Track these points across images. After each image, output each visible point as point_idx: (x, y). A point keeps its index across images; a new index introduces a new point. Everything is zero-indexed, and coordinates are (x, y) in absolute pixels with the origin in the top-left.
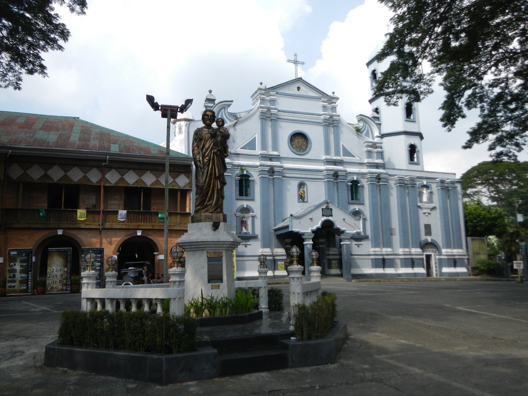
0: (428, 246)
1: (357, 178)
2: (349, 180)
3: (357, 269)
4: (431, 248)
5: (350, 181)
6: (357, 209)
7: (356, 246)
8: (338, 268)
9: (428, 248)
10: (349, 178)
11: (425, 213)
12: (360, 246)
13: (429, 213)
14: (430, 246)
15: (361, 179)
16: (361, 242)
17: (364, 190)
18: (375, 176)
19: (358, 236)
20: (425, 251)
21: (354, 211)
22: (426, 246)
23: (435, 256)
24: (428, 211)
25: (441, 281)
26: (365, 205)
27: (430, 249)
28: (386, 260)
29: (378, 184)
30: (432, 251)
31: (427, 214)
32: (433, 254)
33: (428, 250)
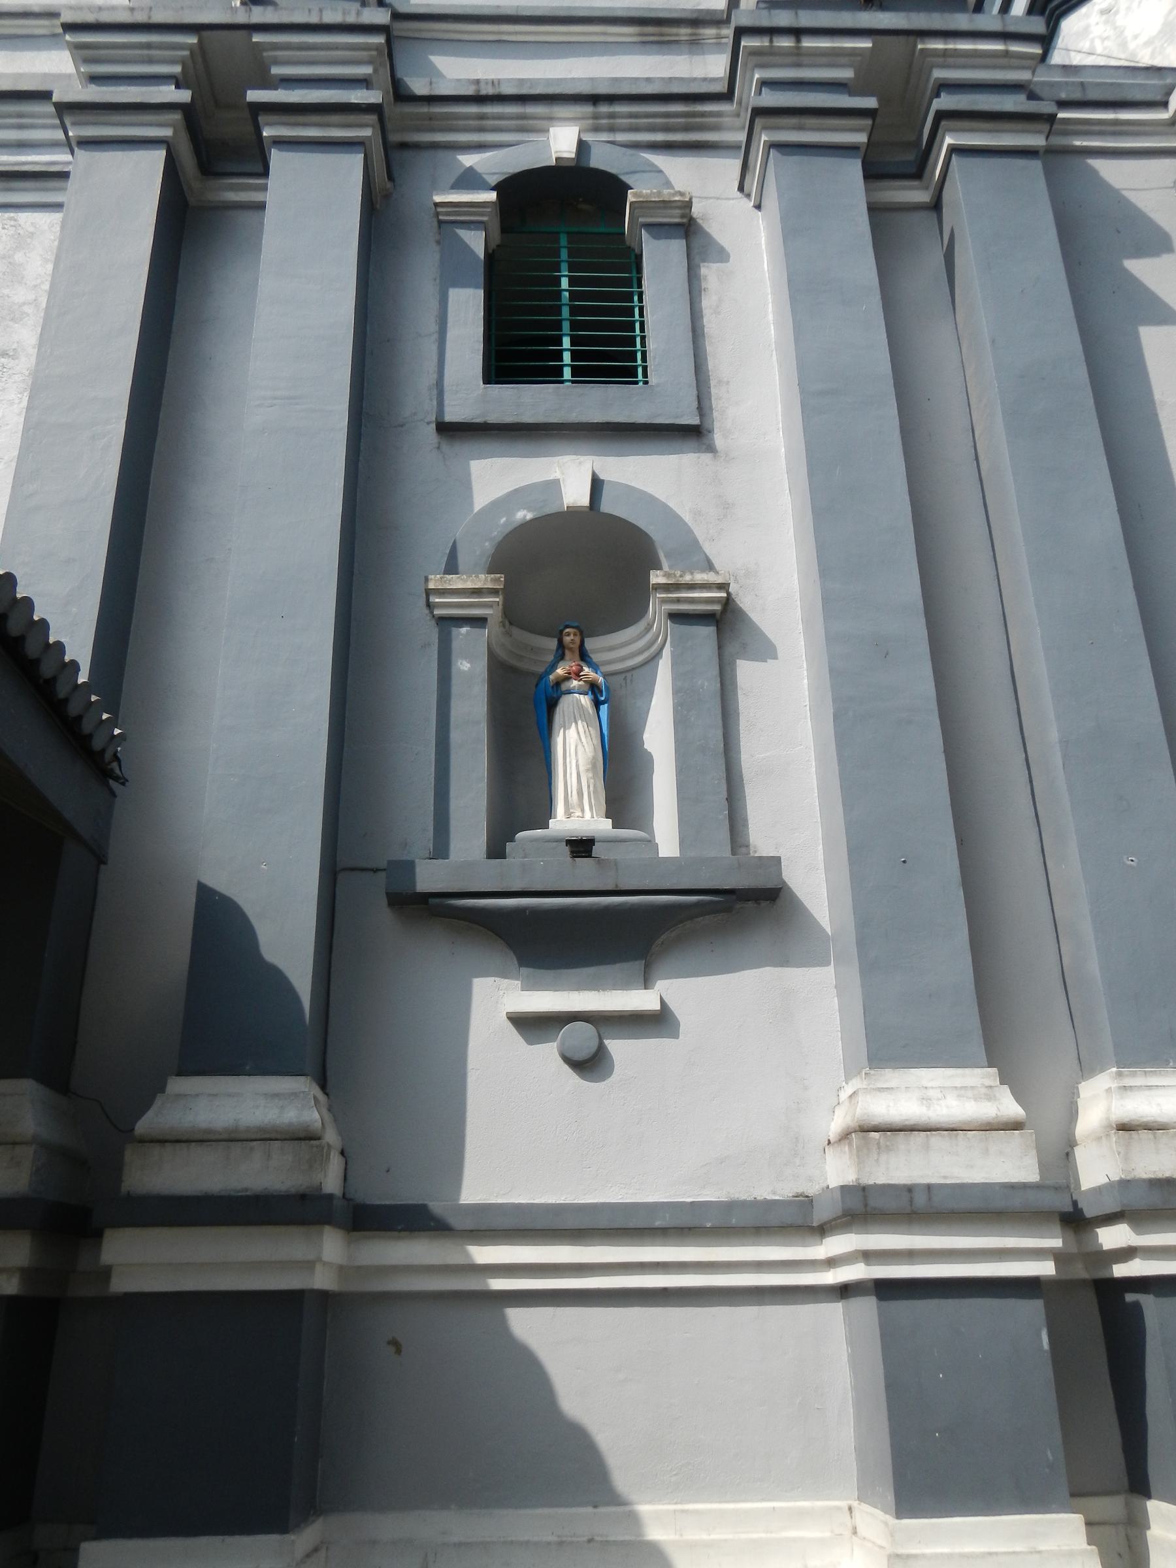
1: (582, 146)
2: (470, 170)
5: (493, 180)
6: (576, 494)
7: (548, 1054)
10: (468, 160)
12: (618, 1048)
15: (659, 160)
16: (647, 984)
17: (709, 272)
18: (847, 74)
19: (584, 874)
21: (524, 515)
26: (718, 439)
28: (1149, 1304)
29: (921, 196)
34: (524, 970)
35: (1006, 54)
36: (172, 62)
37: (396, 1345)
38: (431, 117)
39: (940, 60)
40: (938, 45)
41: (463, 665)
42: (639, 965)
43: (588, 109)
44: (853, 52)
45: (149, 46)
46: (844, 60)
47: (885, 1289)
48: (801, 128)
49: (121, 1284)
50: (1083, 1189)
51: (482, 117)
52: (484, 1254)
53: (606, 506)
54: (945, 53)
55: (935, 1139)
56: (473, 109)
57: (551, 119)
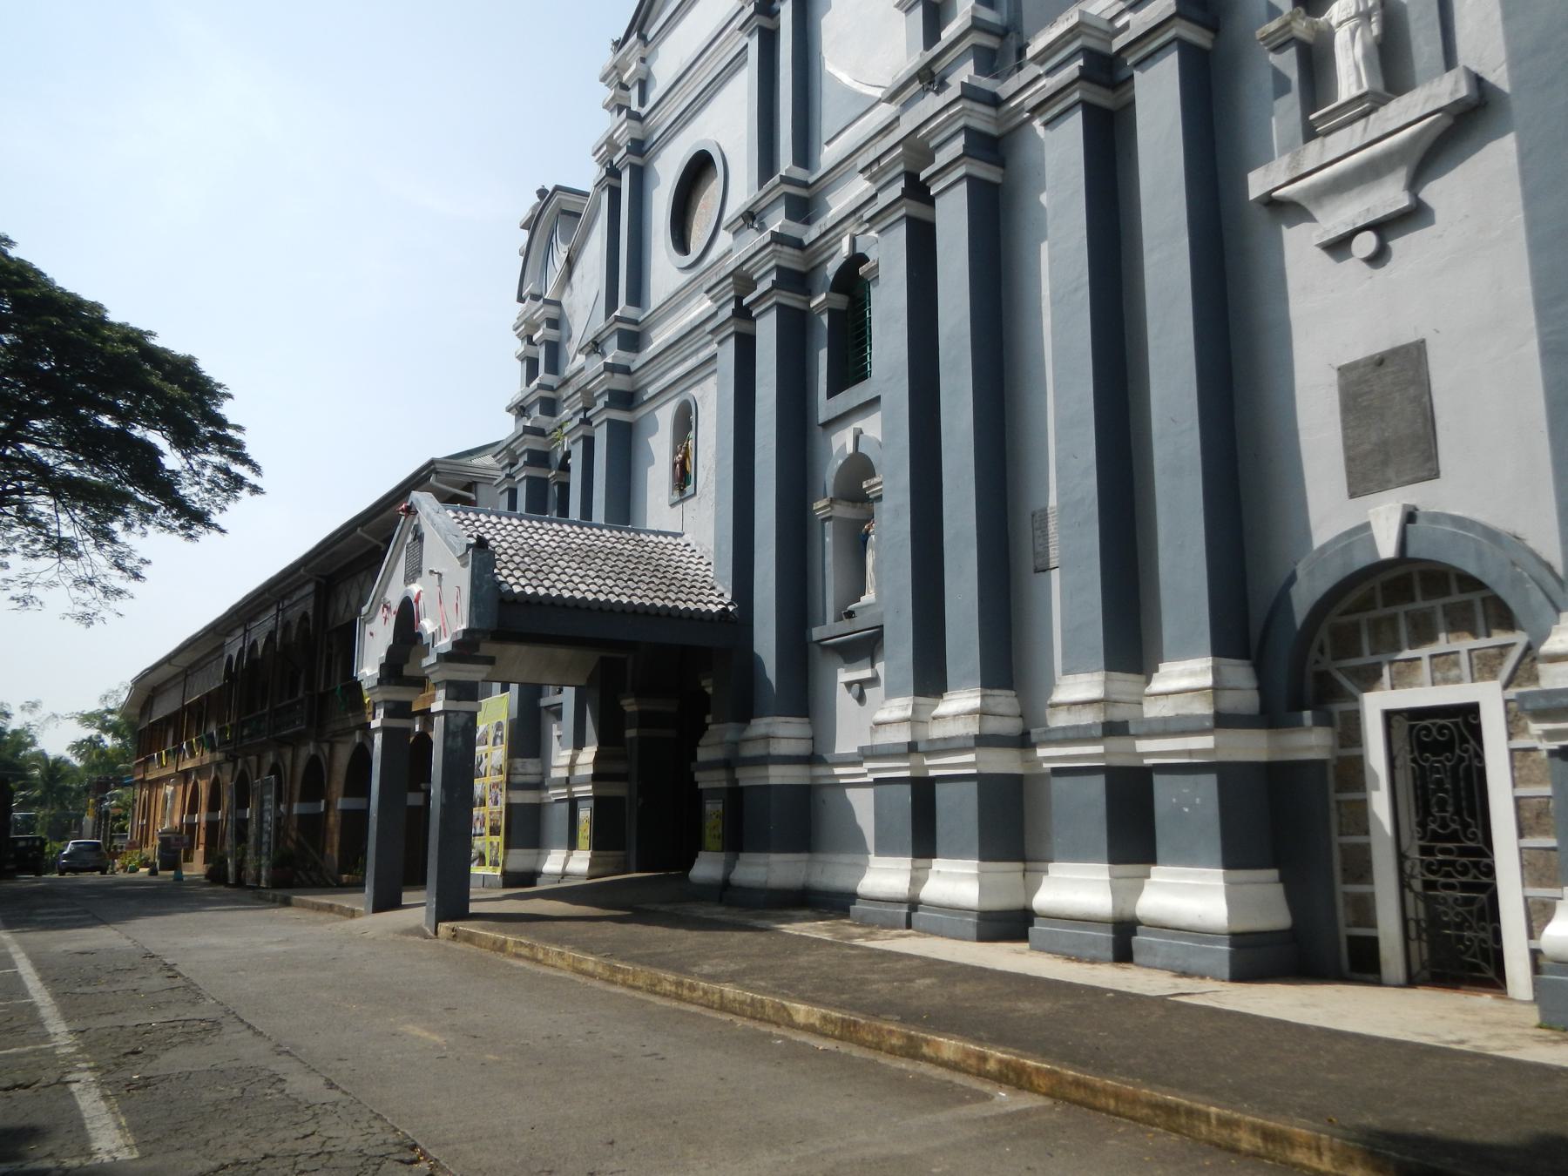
0: (1420, 604)
3: (845, 858)
4: (1461, 622)
8: (722, 851)
9: (1423, 634)
11: (1338, 247)
13: (1385, 227)
14: (1456, 597)
20: (1386, 671)
22: (1401, 610)
23: (1513, 727)
24: (1390, 196)
25: (792, 1025)
27: (1443, 644)
28: (941, 790)
30: (1485, 666)
31: (1366, 244)
32: (1490, 698)
33: (1424, 652)
34: (846, 665)
35: (950, 116)
36: (730, 291)
37: (824, 801)
38: (814, 252)
39: (928, 137)
40: (924, 131)
41: (827, 539)
42: (868, 660)
43: (852, 220)
44: (899, 155)
45: (724, 288)
46: (897, 162)
47: (878, 781)
48: (884, 219)
49: (741, 784)
50: (836, 752)
51: (827, 242)
52: (838, 771)
53: (861, 450)
54: (929, 132)
55: (888, 727)
56: (823, 241)
57: (845, 230)
